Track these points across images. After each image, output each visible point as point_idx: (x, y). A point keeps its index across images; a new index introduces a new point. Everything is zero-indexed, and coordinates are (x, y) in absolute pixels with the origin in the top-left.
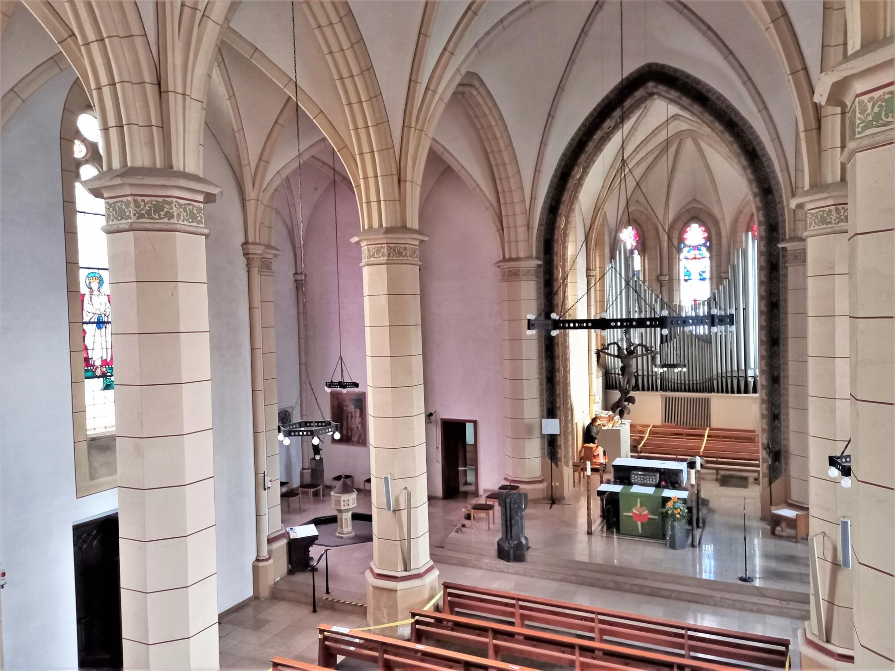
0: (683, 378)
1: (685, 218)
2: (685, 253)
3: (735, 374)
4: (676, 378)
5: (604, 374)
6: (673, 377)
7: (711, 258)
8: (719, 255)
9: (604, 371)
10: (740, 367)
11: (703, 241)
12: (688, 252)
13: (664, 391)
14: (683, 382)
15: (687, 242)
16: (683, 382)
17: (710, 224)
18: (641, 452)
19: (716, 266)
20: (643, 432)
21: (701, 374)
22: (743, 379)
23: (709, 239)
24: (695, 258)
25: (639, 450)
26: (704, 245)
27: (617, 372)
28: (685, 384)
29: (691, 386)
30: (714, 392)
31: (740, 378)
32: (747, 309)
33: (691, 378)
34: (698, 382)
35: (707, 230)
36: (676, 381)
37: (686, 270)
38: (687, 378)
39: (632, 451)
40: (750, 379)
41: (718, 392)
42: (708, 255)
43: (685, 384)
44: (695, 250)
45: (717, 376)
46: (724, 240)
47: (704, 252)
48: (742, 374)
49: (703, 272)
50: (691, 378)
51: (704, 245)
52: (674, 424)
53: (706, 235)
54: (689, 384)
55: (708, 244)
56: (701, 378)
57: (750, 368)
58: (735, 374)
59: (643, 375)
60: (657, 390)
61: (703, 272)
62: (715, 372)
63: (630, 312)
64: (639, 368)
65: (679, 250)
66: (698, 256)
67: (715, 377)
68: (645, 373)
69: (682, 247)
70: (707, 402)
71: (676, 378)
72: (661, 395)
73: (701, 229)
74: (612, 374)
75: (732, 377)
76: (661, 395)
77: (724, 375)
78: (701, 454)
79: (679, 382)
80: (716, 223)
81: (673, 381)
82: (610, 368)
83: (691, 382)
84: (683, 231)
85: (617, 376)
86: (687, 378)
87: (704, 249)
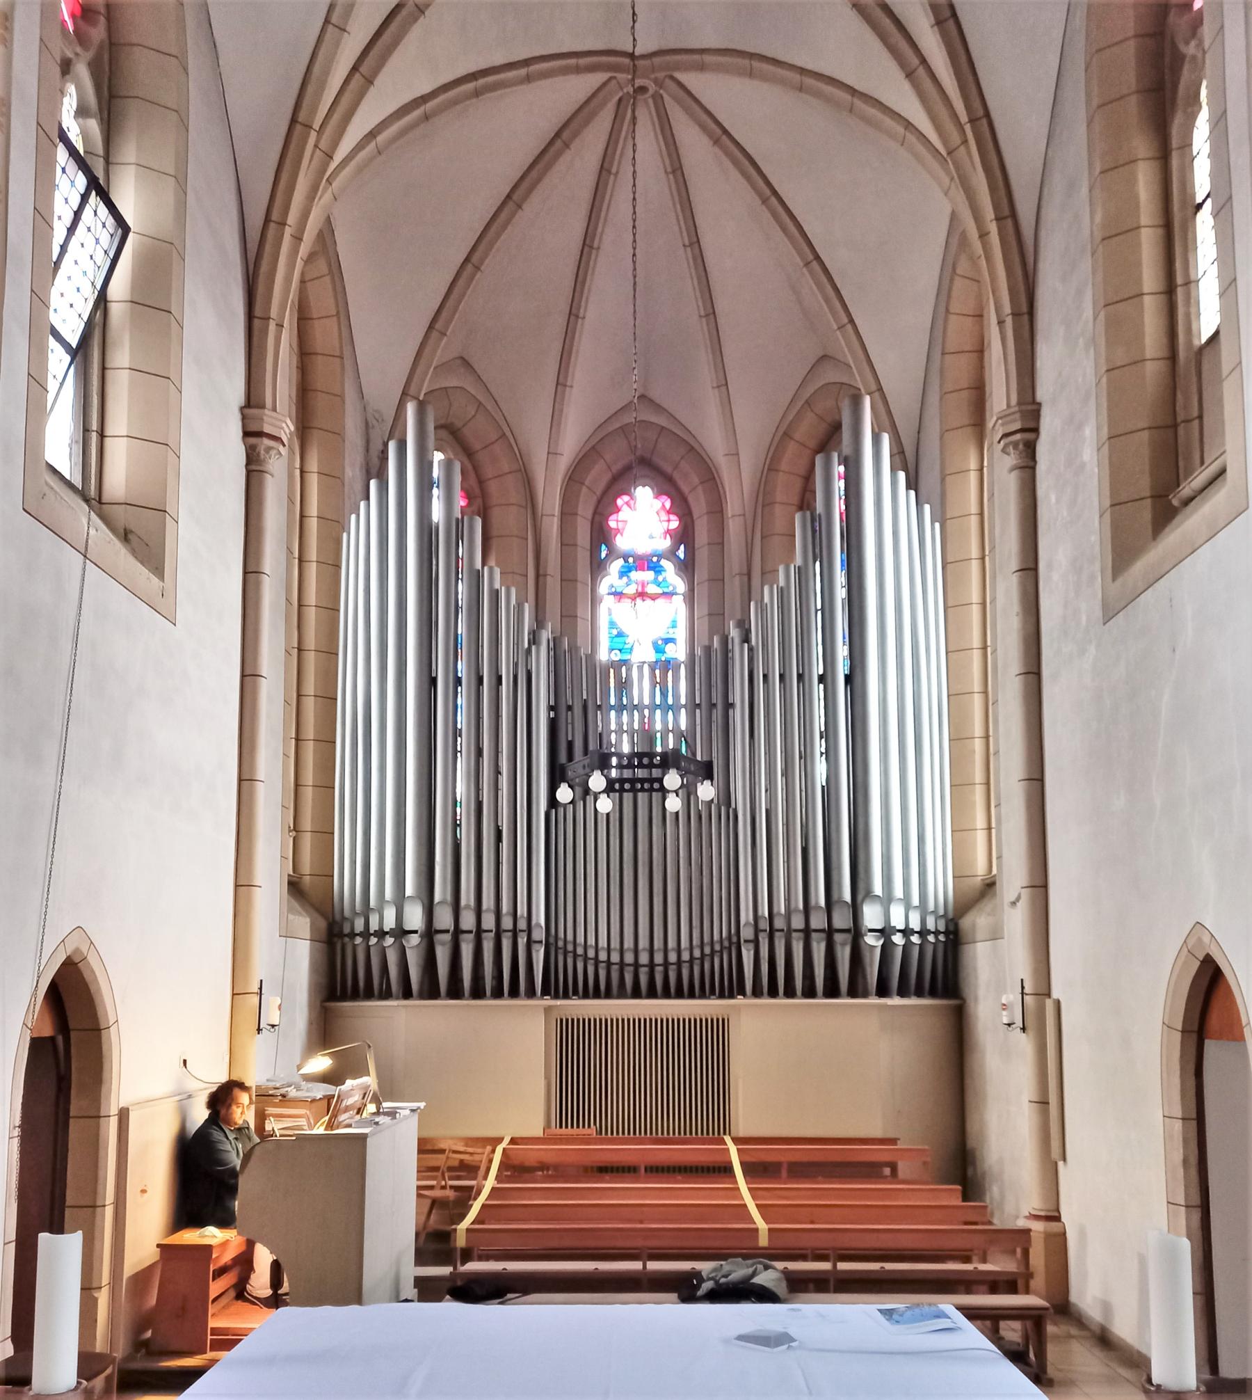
0: (629, 943)
1: (617, 455)
2: (611, 578)
3: (818, 921)
4: (603, 942)
5: (324, 936)
6: (591, 941)
7: (690, 598)
8: (717, 580)
9: (323, 924)
10: (835, 896)
11: (666, 543)
12: (622, 574)
13: (556, 997)
14: (629, 958)
15: (622, 543)
16: (629, 958)
17: (690, 481)
18: (467, 1255)
19: (710, 615)
20: (469, 1169)
21: (696, 922)
22: (848, 937)
23: (684, 536)
24: (642, 595)
25: (461, 1241)
26: (671, 554)
27: (374, 926)
28: (636, 965)
29: (659, 969)
30: (744, 994)
31: (838, 937)
32: (857, 680)
33: (658, 944)
34: (686, 956)
35: (681, 507)
36: (603, 956)
37: (615, 632)
38: (643, 943)
39: (421, 1258)
40: (870, 940)
41: (757, 993)
42: (680, 586)
43: (636, 965)
44: (640, 568)
45: (757, 930)
46: (734, 527)
47: (673, 578)
48: (841, 920)
49: (667, 641)
50: (658, 944)
51: (671, 554)
52: (593, 1131)
53: (675, 524)
54: (652, 966)
55: (681, 553)
56: (696, 942)
57: (869, 894)
58: (818, 921)
59: (479, 932)
60: (531, 993)
61: (667, 641)
62: (746, 915)
63: (433, 681)
64: (463, 902)
65: (598, 567)
66: (652, 589)
67: (747, 933)
68: (489, 922)
69: (603, 555)
70: (718, 1030)
71: (603, 942)
72: (548, 1010)
73: (657, 504)
74: (353, 935)
75: (807, 932)
76: (548, 1010)
77: (779, 923)
78: (763, 1241)
79: (615, 958)
80: (710, 478)
81: (591, 953)
82: (347, 913)
83: (659, 959)
84: (604, 507)
85: (373, 940)
86: (643, 943)
87: (668, 565)
